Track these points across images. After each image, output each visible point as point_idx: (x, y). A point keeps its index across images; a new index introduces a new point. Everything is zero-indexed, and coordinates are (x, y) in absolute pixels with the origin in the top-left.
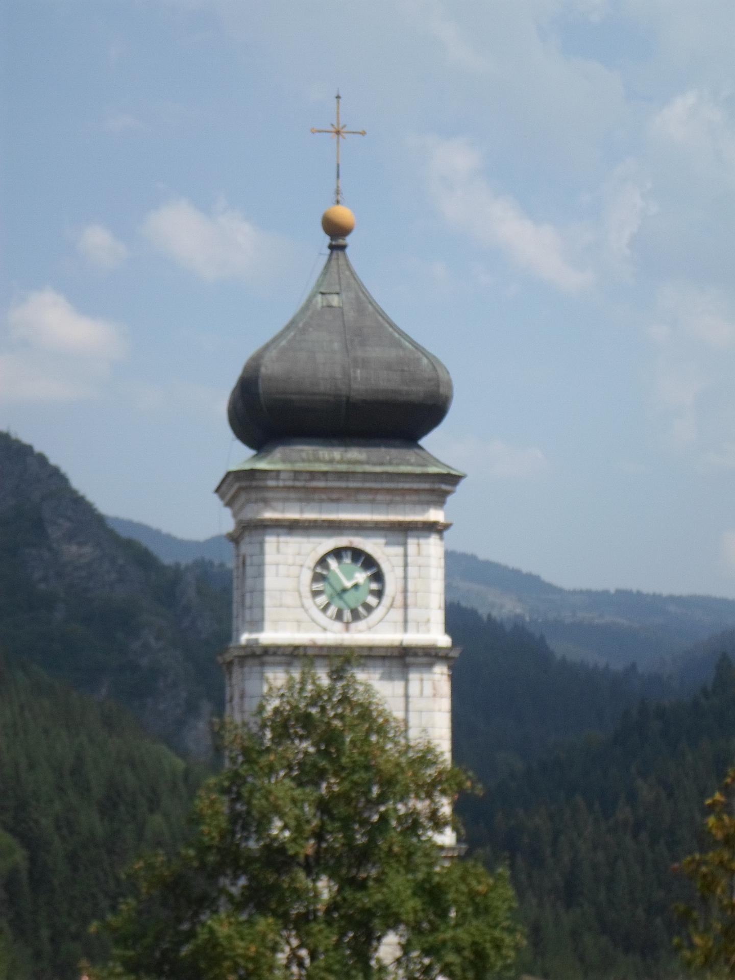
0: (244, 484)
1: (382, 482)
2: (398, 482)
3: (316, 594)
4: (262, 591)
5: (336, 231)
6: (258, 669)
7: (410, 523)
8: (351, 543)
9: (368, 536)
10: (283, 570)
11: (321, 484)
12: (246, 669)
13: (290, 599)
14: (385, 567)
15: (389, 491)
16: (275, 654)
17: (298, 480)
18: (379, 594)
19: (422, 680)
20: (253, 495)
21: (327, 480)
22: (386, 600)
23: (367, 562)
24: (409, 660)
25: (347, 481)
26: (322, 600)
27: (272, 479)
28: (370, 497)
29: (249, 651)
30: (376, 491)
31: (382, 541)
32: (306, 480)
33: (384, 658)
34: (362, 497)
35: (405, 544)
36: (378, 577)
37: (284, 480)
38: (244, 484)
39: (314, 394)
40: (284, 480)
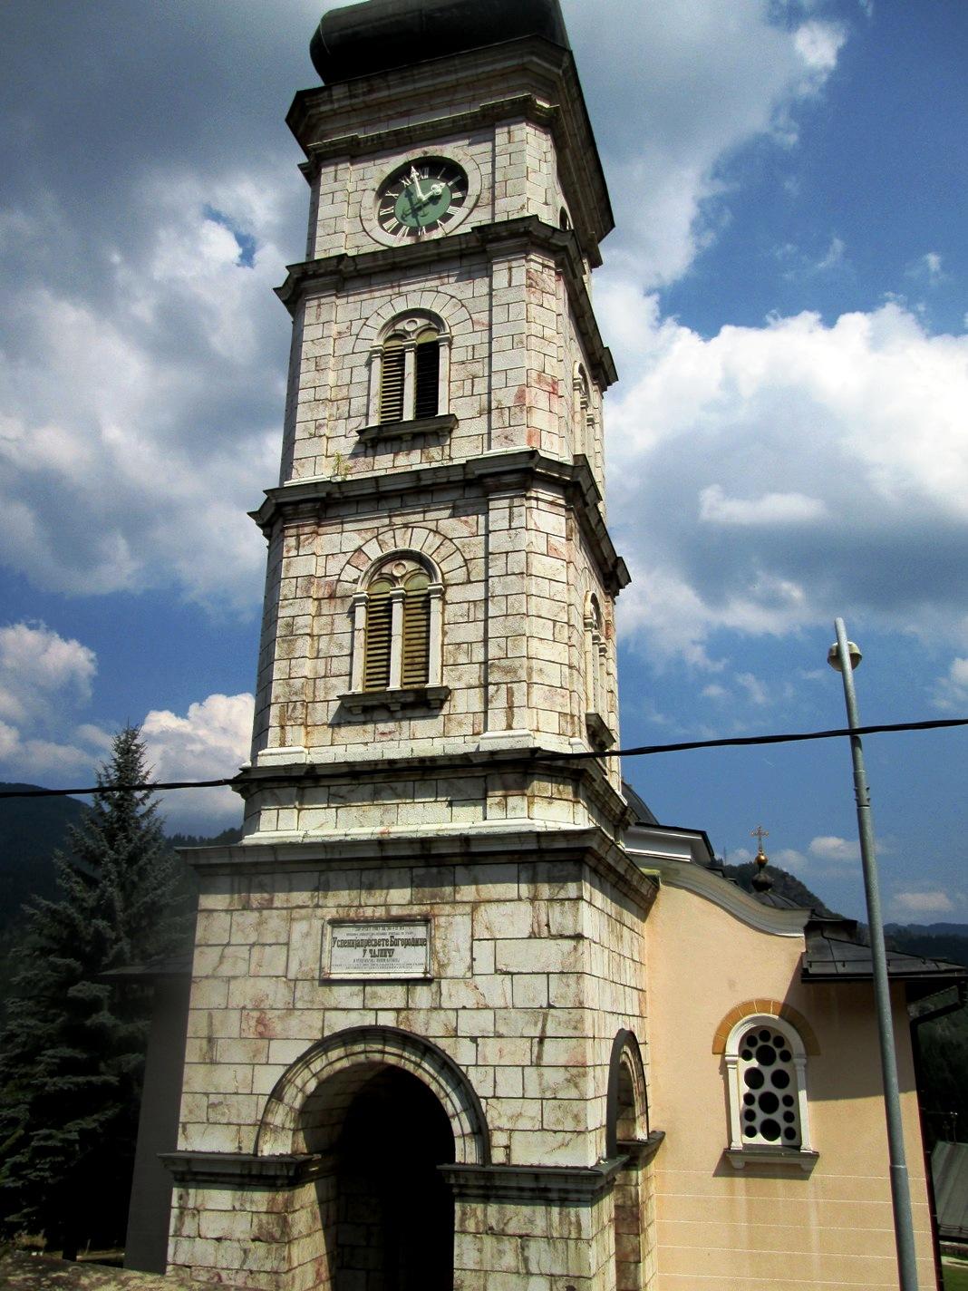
1: (456, 71)
2: (477, 66)
3: (382, 220)
7: (493, 106)
8: (426, 153)
9: (448, 142)
10: (340, 196)
14: (468, 167)
16: (315, 276)
17: (356, 96)
19: (510, 269)
21: (389, 87)
24: (489, 247)
25: (414, 81)
26: (393, 222)
27: (325, 103)
28: (447, 99)
30: (453, 89)
31: (467, 142)
32: (364, 94)
35: (493, 140)
37: (338, 100)
39: (382, 19)
40: (338, 100)
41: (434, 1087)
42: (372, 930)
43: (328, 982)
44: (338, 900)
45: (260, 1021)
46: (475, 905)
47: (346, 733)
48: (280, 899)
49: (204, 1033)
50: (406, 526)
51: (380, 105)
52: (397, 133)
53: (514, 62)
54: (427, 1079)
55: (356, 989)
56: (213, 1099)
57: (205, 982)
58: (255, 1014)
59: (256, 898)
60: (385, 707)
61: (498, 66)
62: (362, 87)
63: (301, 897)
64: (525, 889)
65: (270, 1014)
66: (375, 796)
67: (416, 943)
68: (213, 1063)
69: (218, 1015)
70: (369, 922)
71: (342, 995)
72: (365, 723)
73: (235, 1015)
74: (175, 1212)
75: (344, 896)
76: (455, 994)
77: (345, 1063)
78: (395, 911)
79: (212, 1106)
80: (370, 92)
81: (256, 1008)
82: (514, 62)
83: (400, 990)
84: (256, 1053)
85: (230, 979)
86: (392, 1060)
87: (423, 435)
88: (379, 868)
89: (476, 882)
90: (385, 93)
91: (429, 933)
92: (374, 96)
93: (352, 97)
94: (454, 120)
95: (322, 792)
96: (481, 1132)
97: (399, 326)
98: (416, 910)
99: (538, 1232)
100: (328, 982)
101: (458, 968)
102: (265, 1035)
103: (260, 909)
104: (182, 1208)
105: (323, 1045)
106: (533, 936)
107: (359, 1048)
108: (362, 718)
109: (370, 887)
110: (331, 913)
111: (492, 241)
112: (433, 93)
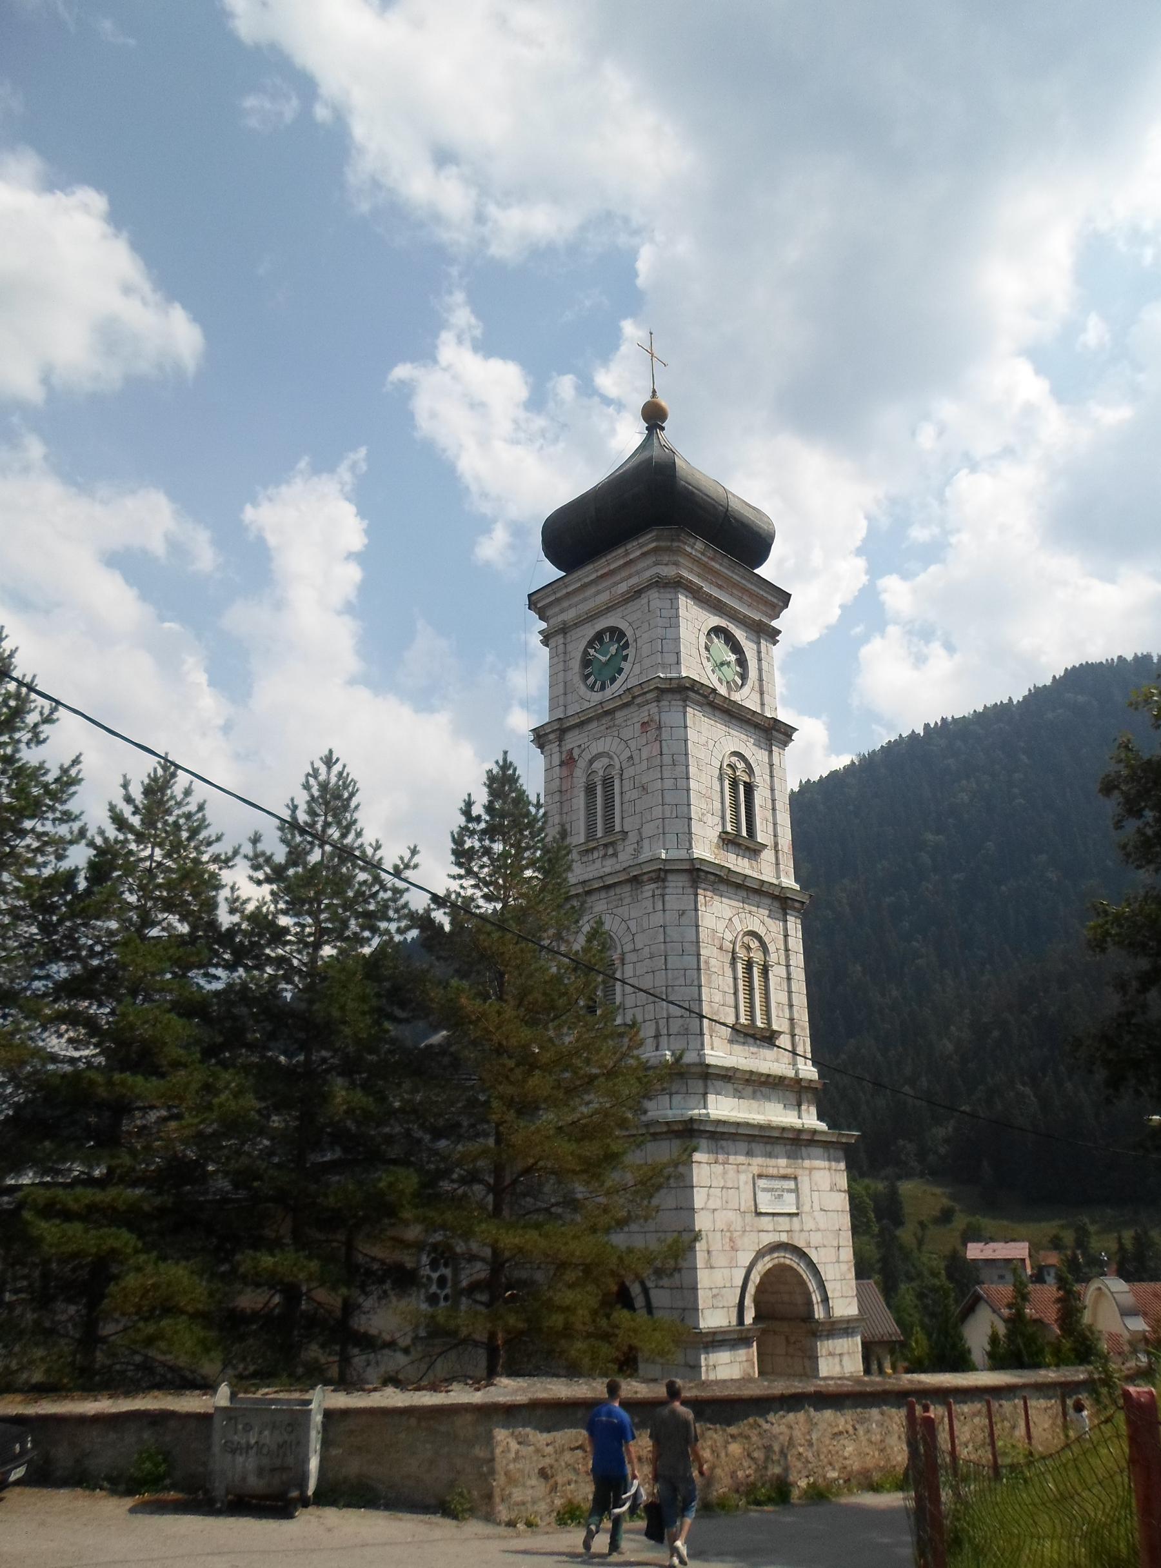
0: (663, 544)
4: (677, 639)
5: (654, 416)
6: (681, 703)
11: (717, 566)
12: (663, 703)
13: (694, 652)
15: (751, 594)
16: (697, 692)
18: (744, 677)
20: (666, 559)
21: (721, 565)
22: (750, 683)
23: (736, 648)
24: (774, 733)
29: (674, 684)
33: (756, 726)
34: (735, 592)
36: (742, 662)
38: (663, 544)
41: (805, 1277)
42: (773, 1182)
43: (759, 1214)
44: (758, 1163)
45: (731, 1240)
46: (811, 1169)
47: (737, 1048)
48: (732, 1158)
49: (705, 1248)
50: (750, 912)
51: (717, 573)
52: (720, 601)
53: (775, 601)
54: (802, 1272)
55: (770, 1218)
56: (715, 1291)
57: (702, 1212)
58: (728, 1234)
59: (721, 1157)
60: (753, 1036)
61: (770, 598)
62: (710, 553)
63: (741, 1159)
64: (826, 1164)
65: (736, 1234)
66: (754, 1097)
67: (790, 1191)
68: (712, 1268)
69: (710, 1234)
70: (772, 1177)
71: (765, 1222)
72: (744, 1044)
73: (719, 1234)
74: (703, 1369)
75: (759, 1160)
76: (809, 1224)
77: (770, 1265)
78: (782, 1172)
79: (714, 1296)
80: (712, 559)
81: (729, 1231)
82: (775, 601)
83: (787, 1219)
84: (732, 1259)
85: (714, 1210)
86: (788, 1262)
87: (748, 848)
88: (773, 1144)
89: (810, 1158)
90: (717, 566)
91: (797, 1185)
92: (713, 563)
93: (703, 554)
94: (745, 616)
95: (730, 1086)
96: (825, 1300)
97: (734, 759)
98: (789, 1171)
99: (845, 1351)
100: (759, 1214)
101: (806, 1208)
102: (734, 1249)
103: (724, 1164)
104: (707, 1366)
105: (760, 1254)
106: (831, 1190)
107: (776, 1255)
108: (742, 1040)
109: (770, 1155)
110: (756, 1170)
111: (777, 731)
112: (736, 585)
